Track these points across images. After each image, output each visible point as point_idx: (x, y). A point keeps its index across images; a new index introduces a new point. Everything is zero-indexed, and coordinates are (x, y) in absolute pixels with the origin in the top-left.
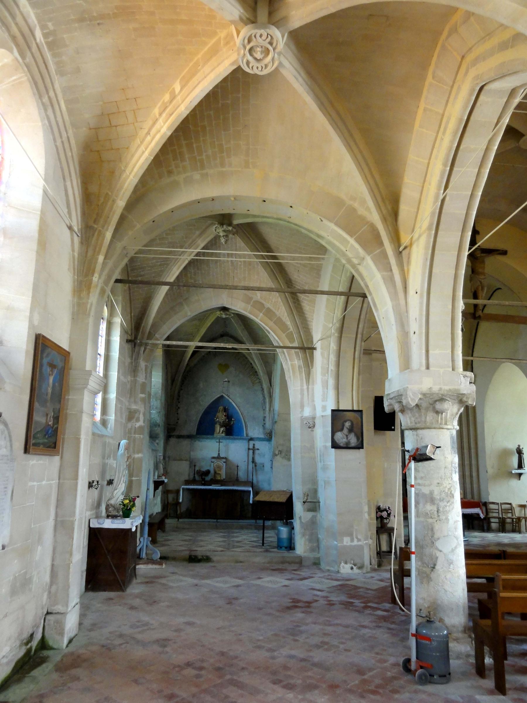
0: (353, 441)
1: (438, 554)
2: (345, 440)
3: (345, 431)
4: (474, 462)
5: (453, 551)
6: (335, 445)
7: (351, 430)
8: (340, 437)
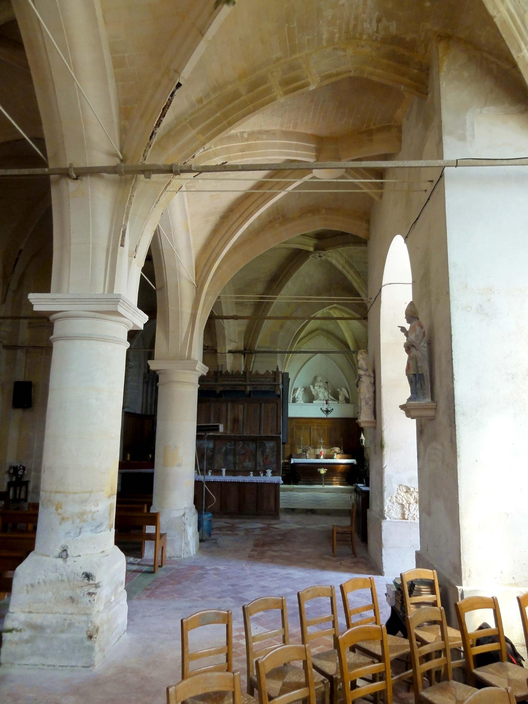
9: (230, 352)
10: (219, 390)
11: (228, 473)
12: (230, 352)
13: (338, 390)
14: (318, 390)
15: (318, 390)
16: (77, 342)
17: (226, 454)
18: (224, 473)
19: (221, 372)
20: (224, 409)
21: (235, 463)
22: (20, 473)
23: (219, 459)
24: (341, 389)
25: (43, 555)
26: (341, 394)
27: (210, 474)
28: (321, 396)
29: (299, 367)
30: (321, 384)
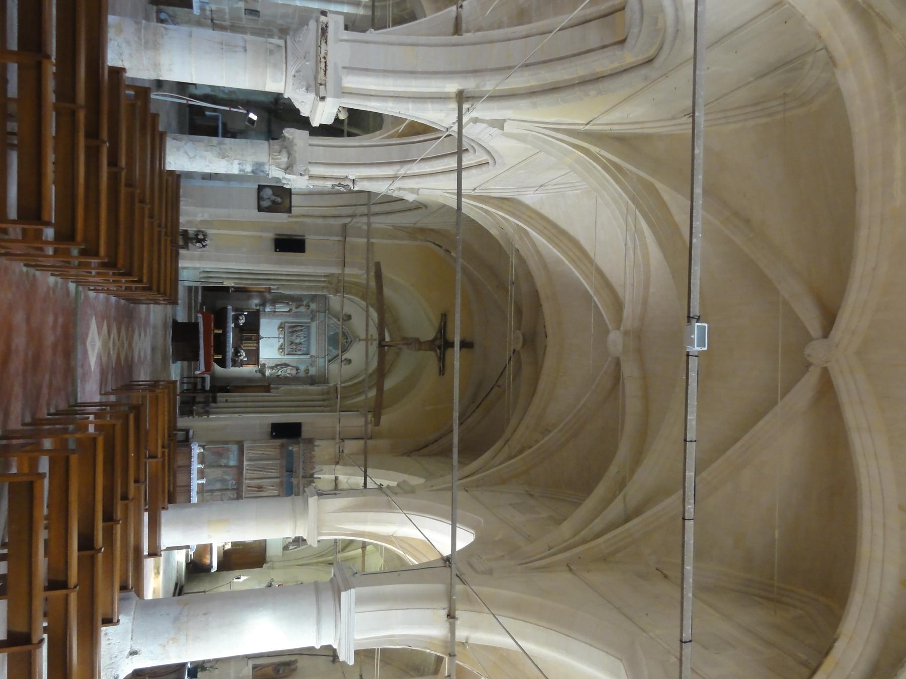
0: (266, 204)
1: (183, 142)
2: (265, 196)
3: (273, 198)
4: (248, 409)
5: (186, 153)
6: (261, 188)
7: (274, 202)
8: (268, 193)
9: (336, 478)
10: (294, 481)
11: (201, 486)
12: (336, 478)
16: (315, 628)
17: (223, 481)
18: (200, 482)
19: (313, 482)
20: (275, 474)
21: (212, 491)
22: (198, 244)
23: (217, 473)
25: (132, 631)
27: (200, 466)
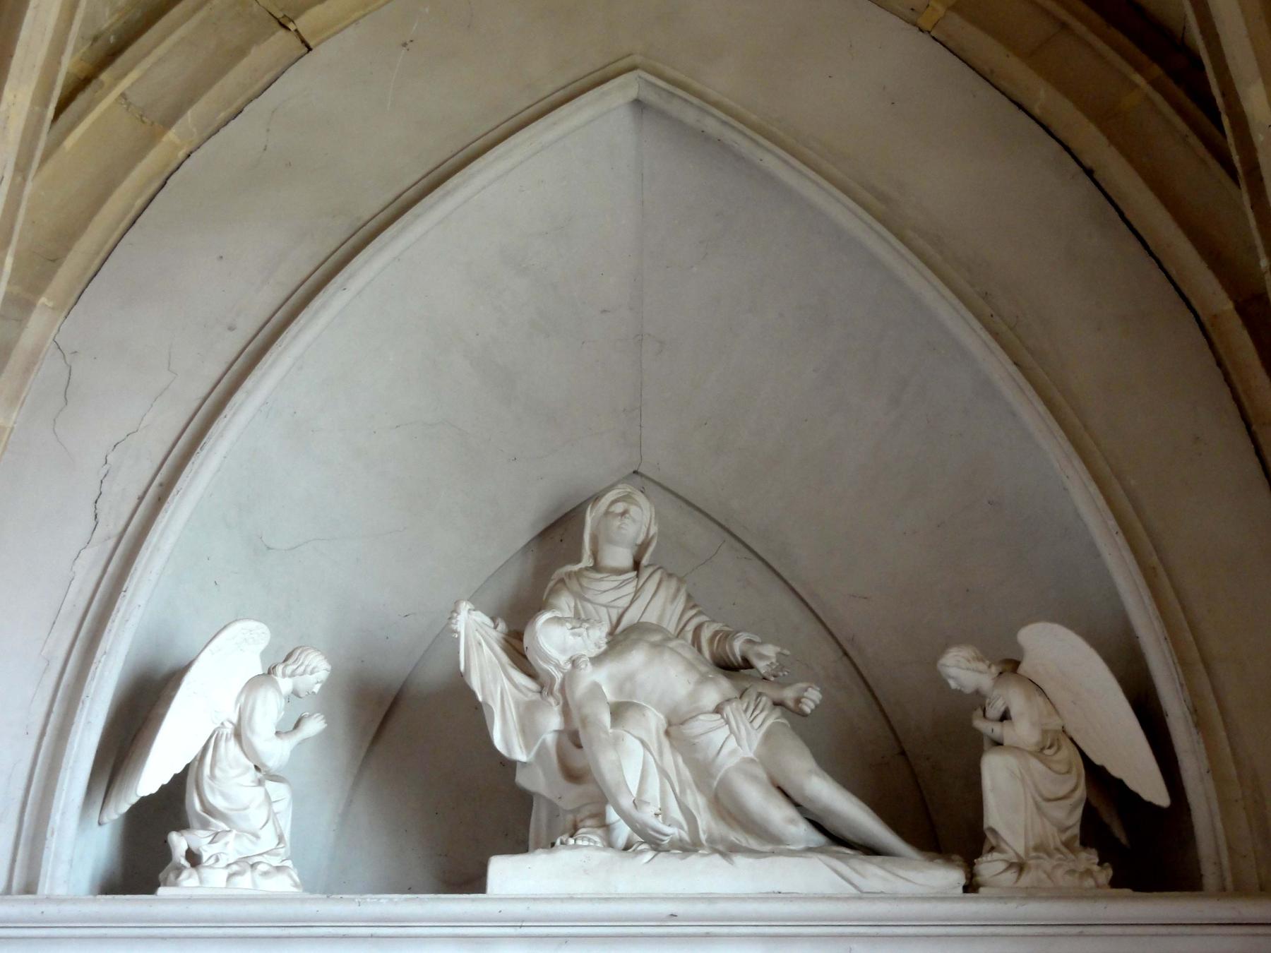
13: (962, 669)
14: (601, 679)
15: (601, 679)
24: (1011, 666)
26: (1023, 731)
28: (634, 766)
29: (263, 302)
30: (659, 604)
